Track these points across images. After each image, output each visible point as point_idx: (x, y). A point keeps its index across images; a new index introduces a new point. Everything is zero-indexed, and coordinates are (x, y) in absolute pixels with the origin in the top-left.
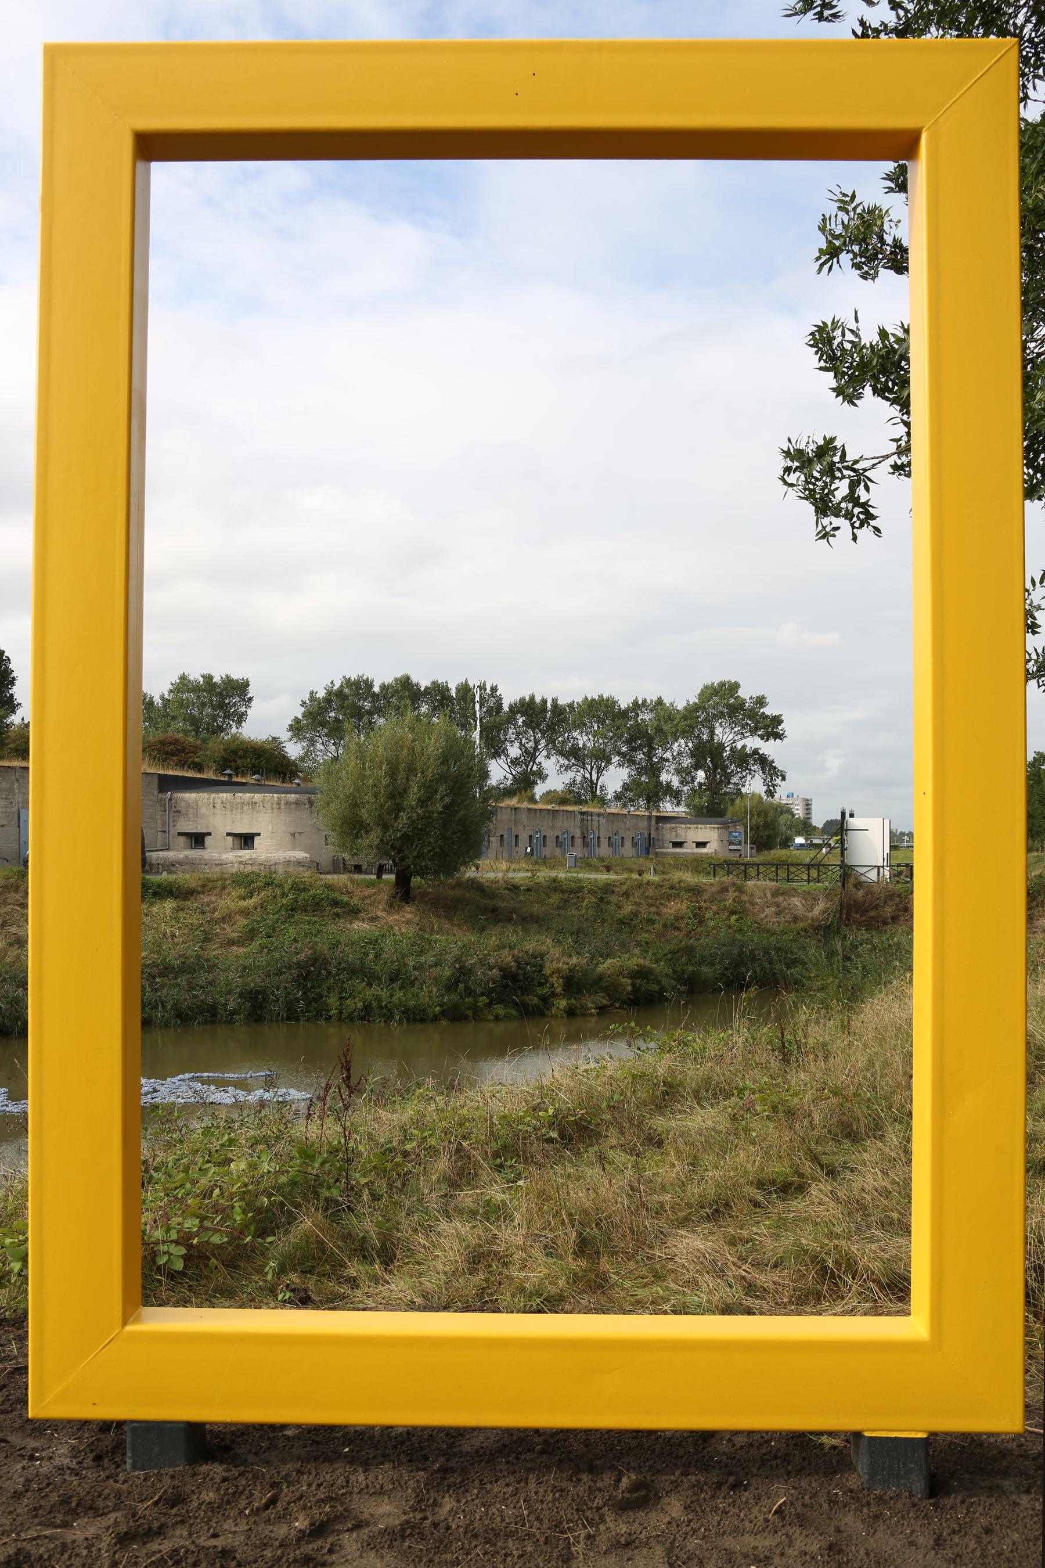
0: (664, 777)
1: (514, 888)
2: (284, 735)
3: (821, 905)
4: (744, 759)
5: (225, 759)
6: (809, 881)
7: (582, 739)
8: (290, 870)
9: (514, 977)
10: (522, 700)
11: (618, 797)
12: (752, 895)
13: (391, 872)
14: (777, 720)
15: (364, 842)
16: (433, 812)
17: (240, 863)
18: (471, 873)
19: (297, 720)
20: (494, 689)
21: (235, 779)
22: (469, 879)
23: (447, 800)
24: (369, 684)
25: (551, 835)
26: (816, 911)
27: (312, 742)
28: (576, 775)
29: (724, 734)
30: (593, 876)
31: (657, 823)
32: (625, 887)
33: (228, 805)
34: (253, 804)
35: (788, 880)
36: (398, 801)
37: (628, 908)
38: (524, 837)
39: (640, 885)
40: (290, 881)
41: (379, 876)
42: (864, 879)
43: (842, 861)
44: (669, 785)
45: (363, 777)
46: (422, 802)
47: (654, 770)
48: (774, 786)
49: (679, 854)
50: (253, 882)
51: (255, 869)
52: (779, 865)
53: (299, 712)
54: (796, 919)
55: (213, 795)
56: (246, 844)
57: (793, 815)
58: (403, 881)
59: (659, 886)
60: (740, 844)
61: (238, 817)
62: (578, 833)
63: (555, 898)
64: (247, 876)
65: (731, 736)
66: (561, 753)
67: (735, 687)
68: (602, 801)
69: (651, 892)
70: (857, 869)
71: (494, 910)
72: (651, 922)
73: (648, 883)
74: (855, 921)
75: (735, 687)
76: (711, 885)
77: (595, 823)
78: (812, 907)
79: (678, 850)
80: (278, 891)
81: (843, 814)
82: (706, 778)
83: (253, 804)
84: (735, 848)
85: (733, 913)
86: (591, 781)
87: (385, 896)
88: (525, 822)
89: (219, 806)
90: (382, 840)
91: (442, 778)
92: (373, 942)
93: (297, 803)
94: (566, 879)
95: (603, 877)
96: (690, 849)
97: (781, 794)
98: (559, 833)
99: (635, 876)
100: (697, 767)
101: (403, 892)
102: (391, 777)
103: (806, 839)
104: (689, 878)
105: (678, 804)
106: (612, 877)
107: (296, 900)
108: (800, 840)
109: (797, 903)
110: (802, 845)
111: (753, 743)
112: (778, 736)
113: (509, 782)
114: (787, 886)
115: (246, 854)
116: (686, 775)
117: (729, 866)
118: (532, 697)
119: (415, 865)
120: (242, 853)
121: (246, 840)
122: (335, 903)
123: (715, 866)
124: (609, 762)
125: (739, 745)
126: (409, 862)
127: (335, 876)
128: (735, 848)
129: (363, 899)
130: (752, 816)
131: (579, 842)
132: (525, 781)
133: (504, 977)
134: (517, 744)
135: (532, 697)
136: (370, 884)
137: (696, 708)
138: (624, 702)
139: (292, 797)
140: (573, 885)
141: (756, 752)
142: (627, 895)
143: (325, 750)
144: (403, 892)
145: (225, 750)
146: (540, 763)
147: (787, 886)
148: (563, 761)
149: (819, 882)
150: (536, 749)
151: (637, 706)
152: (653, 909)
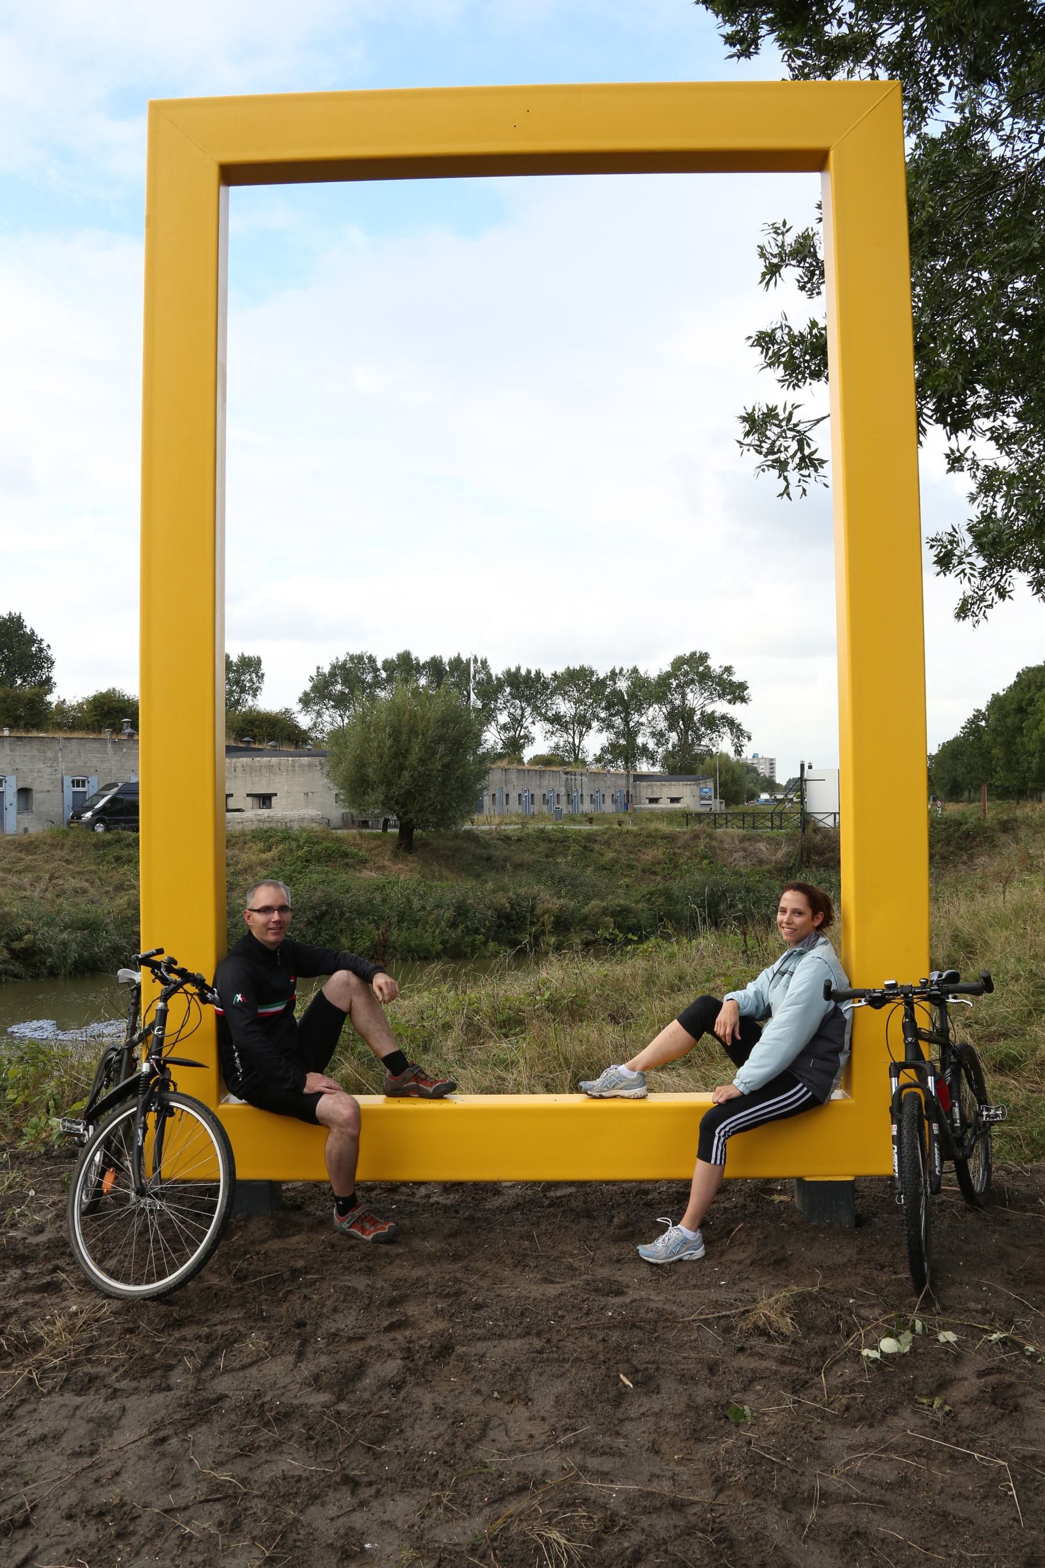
0: (640, 740)
1: (507, 839)
2: (296, 707)
3: (784, 849)
4: (711, 722)
5: (243, 730)
6: (772, 828)
7: (564, 707)
8: (305, 825)
9: (508, 917)
10: (508, 672)
11: (598, 760)
12: (721, 841)
13: (395, 827)
14: (743, 686)
15: (371, 798)
16: (432, 770)
17: (260, 821)
18: (468, 826)
19: (306, 694)
20: (484, 663)
21: (252, 746)
22: (465, 832)
23: (446, 760)
24: (372, 660)
25: (538, 793)
26: (780, 854)
27: (319, 714)
28: (561, 739)
29: (695, 699)
30: (577, 827)
31: (635, 781)
32: (606, 837)
33: (248, 769)
34: (270, 768)
35: (754, 828)
36: (401, 760)
37: (610, 855)
38: (514, 795)
39: (620, 834)
40: (304, 835)
41: (385, 829)
42: (821, 824)
43: (802, 809)
44: (645, 748)
45: (367, 740)
46: (423, 761)
47: (631, 734)
48: (741, 746)
49: (655, 809)
50: (271, 837)
51: (273, 825)
52: (744, 815)
53: (308, 686)
54: (761, 862)
55: (234, 760)
56: (264, 803)
57: (759, 774)
58: (406, 831)
59: (636, 835)
60: (710, 799)
61: (257, 779)
62: (563, 791)
63: (543, 847)
64: (266, 832)
65: (702, 700)
66: (547, 719)
67: (704, 657)
68: (584, 762)
69: (630, 840)
70: (815, 815)
71: (488, 859)
72: (631, 867)
73: (628, 832)
74: (815, 863)
75: (704, 657)
76: (685, 833)
77: (578, 782)
78: (776, 850)
79: (654, 806)
80: (294, 844)
81: (802, 766)
82: (680, 740)
83: (270, 768)
84: (706, 802)
85: (705, 857)
86: (574, 744)
87: (390, 847)
88: (515, 781)
89: (239, 769)
90: (386, 796)
91: (441, 739)
92: (380, 888)
93: (310, 766)
94: (553, 830)
95: (586, 828)
96: (665, 805)
97: (747, 754)
98: (545, 791)
100: (672, 728)
101: (406, 843)
102: (394, 740)
103: (771, 795)
104: (664, 827)
105: (653, 765)
106: (595, 827)
107: (310, 852)
108: (765, 796)
109: (763, 848)
110: (766, 800)
111: (721, 707)
112: (743, 700)
113: (500, 745)
114: (753, 832)
115: (264, 813)
116: (659, 737)
117: (699, 817)
118: (518, 669)
119: (417, 818)
120: (261, 811)
121: (265, 800)
122: (346, 855)
123: (687, 816)
124: (589, 727)
125: (709, 709)
126: (411, 815)
127: (345, 831)
128: (706, 802)
129: (370, 850)
130: (721, 773)
131: (563, 799)
132: (515, 745)
133: (499, 917)
134: (505, 713)
135: (518, 669)
136: (377, 837)
137: (669, 676)
138: (602, 672)
139: (305, 760)
140: (560, 835)
142: (607, 844)
143: (332, 719)
144: (406, 843)
145: (243, 721)
146: (526, 728)
147: (753, 832)
148: (548, 727)
149: (781, 828)
150: (522, 716)
151: (614, 675)
152: (632, 856)
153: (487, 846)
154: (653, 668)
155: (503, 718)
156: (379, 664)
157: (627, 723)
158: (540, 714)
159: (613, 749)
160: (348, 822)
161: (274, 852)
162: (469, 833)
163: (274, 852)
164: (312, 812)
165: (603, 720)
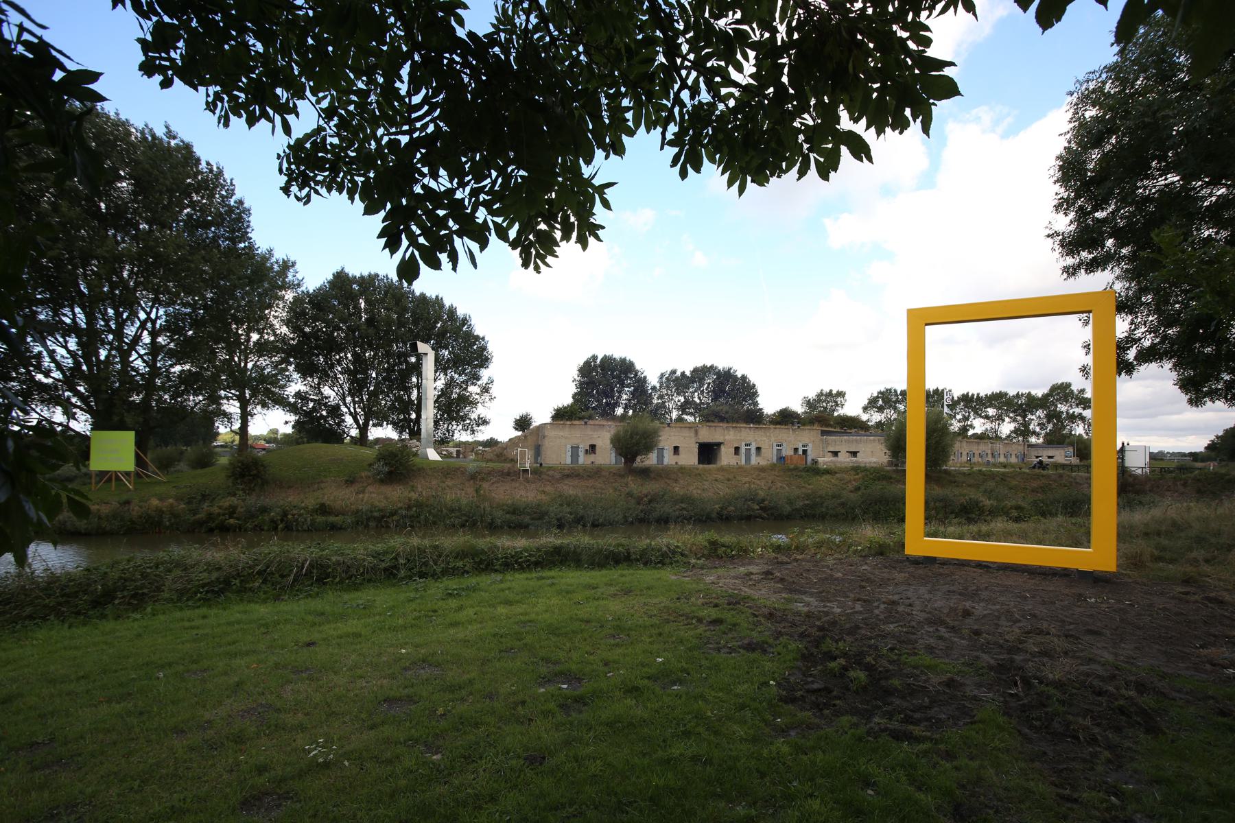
0: (1031, 427)
9: (965, 507)
18: (945, 468)
28: (988, 426)
34: (856, 441)
53: (866, 402)
83: (856, 441)
93: (874, 440)
99: (1018, 470)
115: (854, 459)
116: (1042, 425)
121: (854, 454)
124: (1003, 421)
130: (1077, 445)
132: (964, 430)
138: (1012, 393)
141: (1080, 414)
151: (1018, 396)
153: (954, 476)
154: (1039, 392)
155: (959, 417)
156: (899, 392)
157: (1024, 420)
158: (978, 414)
159: (1016, 431)
160: (890, 464)
161: (860, 475)
162: (945, 470)
163: (860, 475)
164: (874, 460)
165: (1011, 418)
